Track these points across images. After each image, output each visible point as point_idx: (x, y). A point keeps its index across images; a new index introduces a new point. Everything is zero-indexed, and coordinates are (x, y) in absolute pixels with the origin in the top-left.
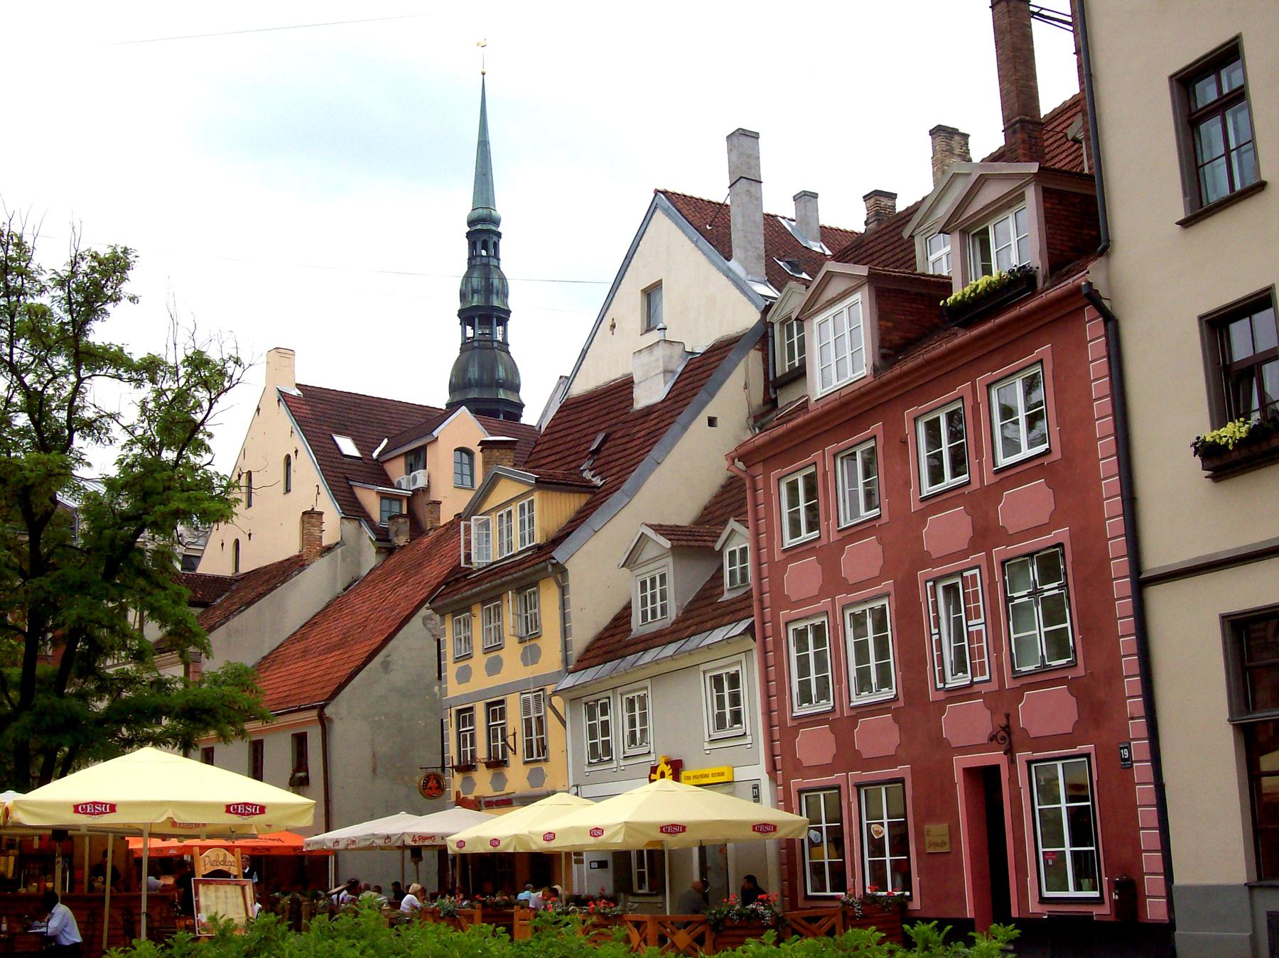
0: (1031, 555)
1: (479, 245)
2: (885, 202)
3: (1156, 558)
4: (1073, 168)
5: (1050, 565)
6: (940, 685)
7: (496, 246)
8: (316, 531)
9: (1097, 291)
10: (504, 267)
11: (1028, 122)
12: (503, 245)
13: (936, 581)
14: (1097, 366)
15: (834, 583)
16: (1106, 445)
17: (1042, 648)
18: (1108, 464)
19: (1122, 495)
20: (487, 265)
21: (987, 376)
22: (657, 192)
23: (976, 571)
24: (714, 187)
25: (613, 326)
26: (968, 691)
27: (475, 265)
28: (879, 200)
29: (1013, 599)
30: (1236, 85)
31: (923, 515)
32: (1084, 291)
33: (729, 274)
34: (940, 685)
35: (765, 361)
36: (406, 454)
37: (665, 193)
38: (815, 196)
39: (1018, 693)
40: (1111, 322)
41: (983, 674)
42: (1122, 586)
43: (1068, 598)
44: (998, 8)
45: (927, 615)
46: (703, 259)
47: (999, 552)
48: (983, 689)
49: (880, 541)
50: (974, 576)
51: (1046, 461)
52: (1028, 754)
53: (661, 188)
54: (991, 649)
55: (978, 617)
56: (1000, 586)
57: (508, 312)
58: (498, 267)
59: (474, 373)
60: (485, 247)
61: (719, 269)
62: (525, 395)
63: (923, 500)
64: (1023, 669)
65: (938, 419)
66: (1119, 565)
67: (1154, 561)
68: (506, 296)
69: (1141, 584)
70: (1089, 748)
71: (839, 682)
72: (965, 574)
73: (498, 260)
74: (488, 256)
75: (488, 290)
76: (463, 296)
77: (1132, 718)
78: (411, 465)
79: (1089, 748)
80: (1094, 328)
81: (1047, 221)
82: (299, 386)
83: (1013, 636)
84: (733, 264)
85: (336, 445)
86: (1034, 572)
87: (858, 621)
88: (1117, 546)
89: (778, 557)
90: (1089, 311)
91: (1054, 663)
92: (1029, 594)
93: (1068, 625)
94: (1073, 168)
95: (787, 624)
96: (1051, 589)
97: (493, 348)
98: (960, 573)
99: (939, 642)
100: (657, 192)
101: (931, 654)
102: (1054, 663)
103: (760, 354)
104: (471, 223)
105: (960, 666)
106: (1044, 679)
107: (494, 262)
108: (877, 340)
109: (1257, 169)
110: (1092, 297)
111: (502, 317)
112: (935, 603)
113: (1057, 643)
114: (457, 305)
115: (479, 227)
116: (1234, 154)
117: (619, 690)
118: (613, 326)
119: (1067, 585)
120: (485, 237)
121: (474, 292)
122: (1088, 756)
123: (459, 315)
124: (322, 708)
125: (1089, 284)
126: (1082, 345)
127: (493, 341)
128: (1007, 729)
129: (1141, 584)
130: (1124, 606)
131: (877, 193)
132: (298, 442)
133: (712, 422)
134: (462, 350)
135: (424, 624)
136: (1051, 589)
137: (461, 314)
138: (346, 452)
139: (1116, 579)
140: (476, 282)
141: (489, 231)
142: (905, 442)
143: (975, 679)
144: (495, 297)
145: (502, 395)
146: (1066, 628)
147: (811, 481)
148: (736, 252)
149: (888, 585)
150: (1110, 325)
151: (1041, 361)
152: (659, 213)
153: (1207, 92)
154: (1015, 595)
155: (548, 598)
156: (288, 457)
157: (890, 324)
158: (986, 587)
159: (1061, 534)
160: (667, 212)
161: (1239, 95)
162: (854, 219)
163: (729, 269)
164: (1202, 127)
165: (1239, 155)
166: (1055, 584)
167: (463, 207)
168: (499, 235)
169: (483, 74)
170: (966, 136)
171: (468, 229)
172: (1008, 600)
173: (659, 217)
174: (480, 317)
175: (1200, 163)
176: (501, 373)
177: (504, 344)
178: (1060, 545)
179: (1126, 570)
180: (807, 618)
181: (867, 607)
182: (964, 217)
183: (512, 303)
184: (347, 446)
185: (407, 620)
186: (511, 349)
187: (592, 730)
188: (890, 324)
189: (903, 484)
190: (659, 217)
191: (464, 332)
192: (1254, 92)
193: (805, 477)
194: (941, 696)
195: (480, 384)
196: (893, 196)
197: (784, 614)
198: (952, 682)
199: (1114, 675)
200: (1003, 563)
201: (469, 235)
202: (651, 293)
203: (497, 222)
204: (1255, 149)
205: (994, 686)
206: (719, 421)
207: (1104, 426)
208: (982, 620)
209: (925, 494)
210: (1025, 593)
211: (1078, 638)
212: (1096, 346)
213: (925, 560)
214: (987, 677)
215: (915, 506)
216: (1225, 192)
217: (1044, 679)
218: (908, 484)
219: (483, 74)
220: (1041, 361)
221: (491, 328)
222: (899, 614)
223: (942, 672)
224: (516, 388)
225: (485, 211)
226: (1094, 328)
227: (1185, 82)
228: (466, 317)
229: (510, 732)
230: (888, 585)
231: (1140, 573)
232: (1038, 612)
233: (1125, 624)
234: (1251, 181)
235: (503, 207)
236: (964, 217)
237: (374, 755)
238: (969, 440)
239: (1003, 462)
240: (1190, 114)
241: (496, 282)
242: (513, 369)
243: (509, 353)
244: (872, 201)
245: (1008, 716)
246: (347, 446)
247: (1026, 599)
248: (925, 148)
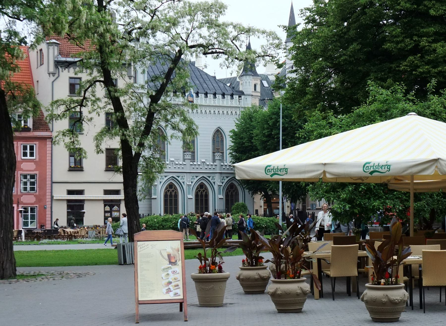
0: (28, 174)
5: (33, 177)
21: (22, 143)
39: (22, 196)
42: (49, 182)
51: (35, 160)
52: (23, 205)
67: (54, 180)
69: (53, 183)
70: (37, 205)
79: (37, 205)
86: (28, 177)
96: (32, 180)
122: (37, 207)
128: (18, 201)
129: (53, 183)
136: (32, 180)
178: (36, 174)
199: (45, 195)
200: (21, 174)
207: (49, 158)
211: (38, 189)
245: (18, 199)
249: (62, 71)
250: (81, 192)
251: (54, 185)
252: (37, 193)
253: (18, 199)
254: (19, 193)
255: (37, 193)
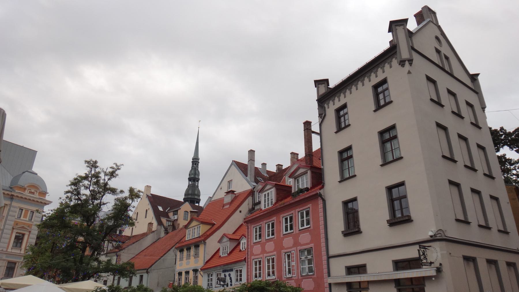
0: (306, 249)
1: (194, 164)
2: (280, 167)
3: (331, 253)
4: (318, 166)
5: (309, 251)
6: (285, 277)
7: (198, 165)
8: (151, 227)
9: (321, 194)
10: (199, 170)
11: (310, 155)
12: (199, 164)
13: (285, 253)
14: (321, 210)
15: (264, 251)
16: (322, 227)
17: (307, 270)
18: (322, 231)
19: (325, 238)
20: (195, 169)
22: (233, 161)
23: (294, 252)
24: (245, 160)
25: (221, 189)
26: (291, 278)
27: (193, 168)
28: (279, 166)
29: (301, 258)
30: (351, 155)
31: (283, 239)
32: (318, 194)
33: (247, 180)
34: (285, 277)
35: (253, 199)
36: (173, 211)
37: (235, 161)
38: (266, 164)
39: (302, 280)
40: (324, 200)
41: (294, 275)
42: (325, 258)
43: (313, 259)
44: (305, 131)
45: (283, 261)
46: (241, 176)
47: (299, 248)
48: (294, 278)
49: (274, 243)
50: (293, 253)
53: (233, 160)
54: (296, 269)
55: (294, 262)
56: (299, 255)
57: (199, 179)
58: (198, 169)
59: (190, 192)
60: (195, 164)
61: (245, 179)
62: (201, 197)
63: (284, 235)
64: (303, 274)
65: (287, 218)
66: (324, 253)
67: (331, 253)
68: (199, 175)
69: (329, 257)
71: (264, 273)
72: (292, 252)
73: (198, 168)
74: (196, 167)
75: (195, 174)
76: (190, 175)
77: (326, 288)
78: (174, 214)
80: (320, 202)
81: (312, 178)
82: (151, 194)
83: (301, 267)
84: (247, 178)
85: (158, 208)
86: (306, 253)
87: (268, 261)
88: (324, 249)
89: (252, 244)
90: (319, 198)
91: (310, 274)
92: (305, 258)
93: (313, 265)
94: (318, 166)
95: (253, 260)
96: (309, 257)
97: (195, 187)
98: (290, 252)
99: (285, 267)
100: (233, 161)
101: (284, 269)
102: (310, 274)
103: (252, 197)
104: (193, 159)
105: (289, 272)
106: (307, 277)
107: (197, 168)
108: (276, 199)
109: (354, 172)
110: (320, 195)
111: (198, 180)
112: (285, 258)
113: (310, 270)
114: (188, 177)
115: (195, 160)
116: (350, 168)
117: (215, 271)
118: (221, 189)
119: (313, 257)
120: (196, 163)
121: (192, 174)
123: (188, 179)
124: (148, 269)
125: (320, 193)
126: (318, 205)
127: (195, 185)
129: (329, 257)
130: (325, 262)
131: (279, 165)
132: (149, 207)
133: (240, 212)
134: (188, 187)
135: (173, 251)
136: (309, 257)
137: (189, 179)
138: (160, 210)
139: (323, 256)
140: (193, 172)
141: (197, 161)
142: (280, 222)
143: (293, 276)
144: (196, 176)
145: (196, 197)
146: (312, 266)
147: (260, 228)
148: (249, 175)
149: (275, 253)
150: (324, 201)
151: (309, 208)
152: (233, 165)
153: (345, 155)
154: (302, 258)
155: (201, 248)
156: (147, 210)
157: (279, 196)
158: (296, 256)
159: (312, 245)
160: (235, 166)
161: (351, 157)
162: (274, 169)
163: (247, 179)
164: (344, 162)
165: (351, 168)
166: (310, 256)
167: (192, 156)
168: (199, 162)
169: (199, 128)
170: (298, 154)
171: (192, 160)
172: (300, 259)
173: (233, 166)
174: (193, 180)
175: (343, 169)
176: (196, 193)
177: (198, 186)
178: (312, 248)
179: (325, 254)
180: (257, 259)
181: (270, 257)
182: (295, 175)
183: (200, 177)
184: (160, 209)
185: (169, 250)
186: (199, 187)
187: (208, 280)
188: (279, 196)
189: (279, 231)
190: (233, 166)
191: (189, 183)
192: (354, 156)
193: (259, 227)
194: (285, 279)
195: (191, 195)
196: (282, 166)
197: (253, 257)
198: (288, 276)
200: (300, 250)
201: (192, 162)
202: (230, 182)
203: (198, 159)
204: (354, 168)
205: (297, 278)
206: (242, 212)
207: (322, 222)
208: (295, 263)
209: (284, 234)
210: (304, 257)
211: (315, 268)
212: (321, 205)
213: (283, 248)
214: (295, 276)
215: (282, 236)
216: (348, 176)
217: (307, 277)
218: (280, 231)
219: (199, 128)
220: (309, 208)
221: (195, 182)
222: (277, 259)
223: (286, 273)
224: (199, 196)
225: (196, 157)
226: (320, 202)
227: (341, 153)
228: (190, 179)
229: (190, 279)
230: (275, 253)
231: (328, 255)
232: (307, 262)
233: (325, 266)
234: (353, 174)
235: (200, 156)
236: (295, 175)
237: (158, 282)
238: (293, 223)
239: (301, 228)
240: (342, 160)
241: (197, 172)
242: (199, 192)
243: (198, 188)
244: (277, 166)
245: (299, 285)
246: (160, 209)
247: (304, 259)
248: (289, 156)
249: (328, 108)
250: (361, 269)
251: (331, 260)
252: (315, 276)
253: (299, 285)
254: (300, 278)
255: (315, 276)
